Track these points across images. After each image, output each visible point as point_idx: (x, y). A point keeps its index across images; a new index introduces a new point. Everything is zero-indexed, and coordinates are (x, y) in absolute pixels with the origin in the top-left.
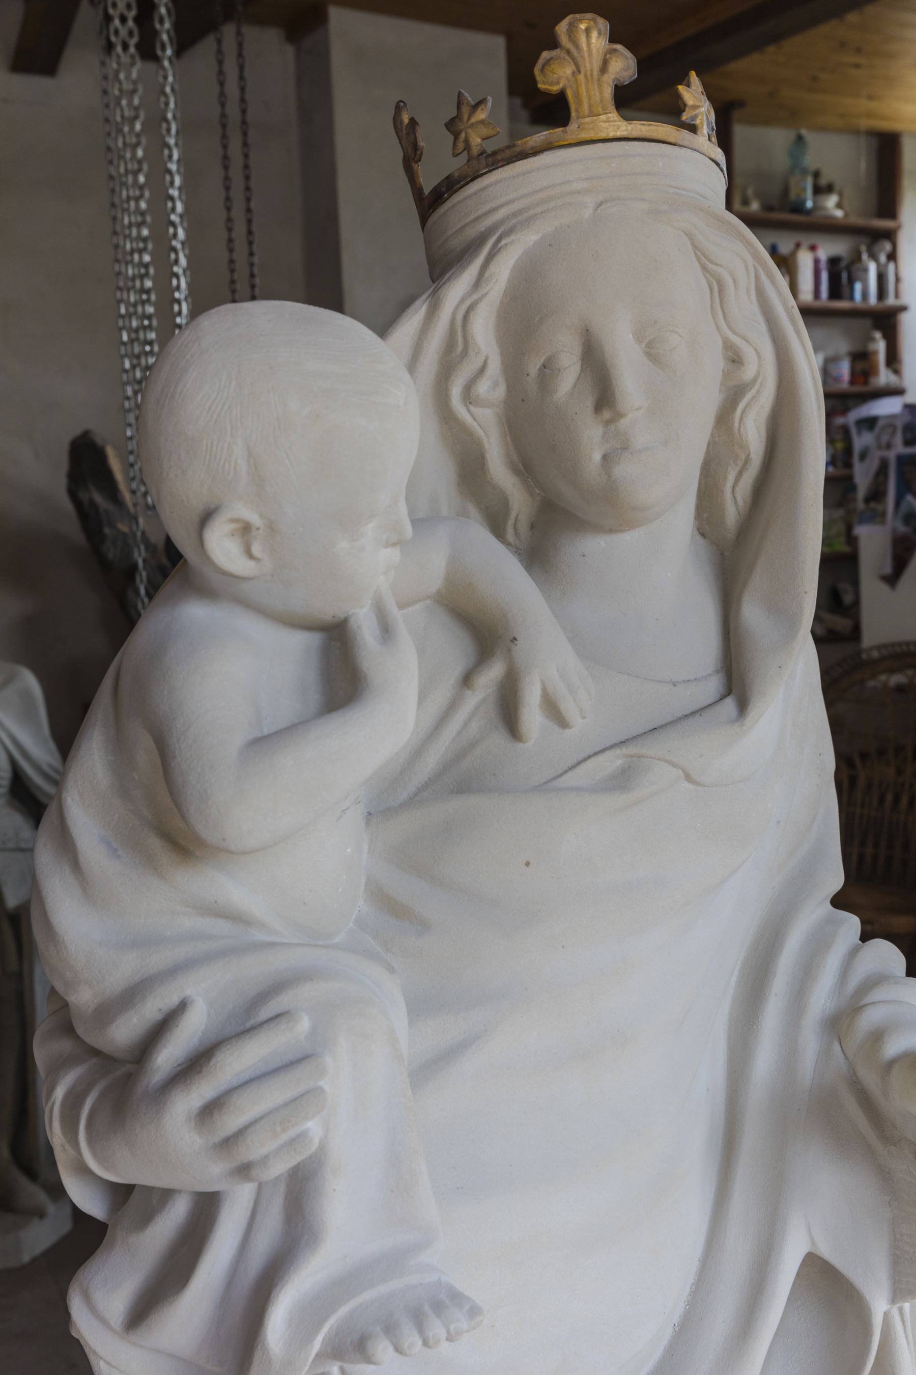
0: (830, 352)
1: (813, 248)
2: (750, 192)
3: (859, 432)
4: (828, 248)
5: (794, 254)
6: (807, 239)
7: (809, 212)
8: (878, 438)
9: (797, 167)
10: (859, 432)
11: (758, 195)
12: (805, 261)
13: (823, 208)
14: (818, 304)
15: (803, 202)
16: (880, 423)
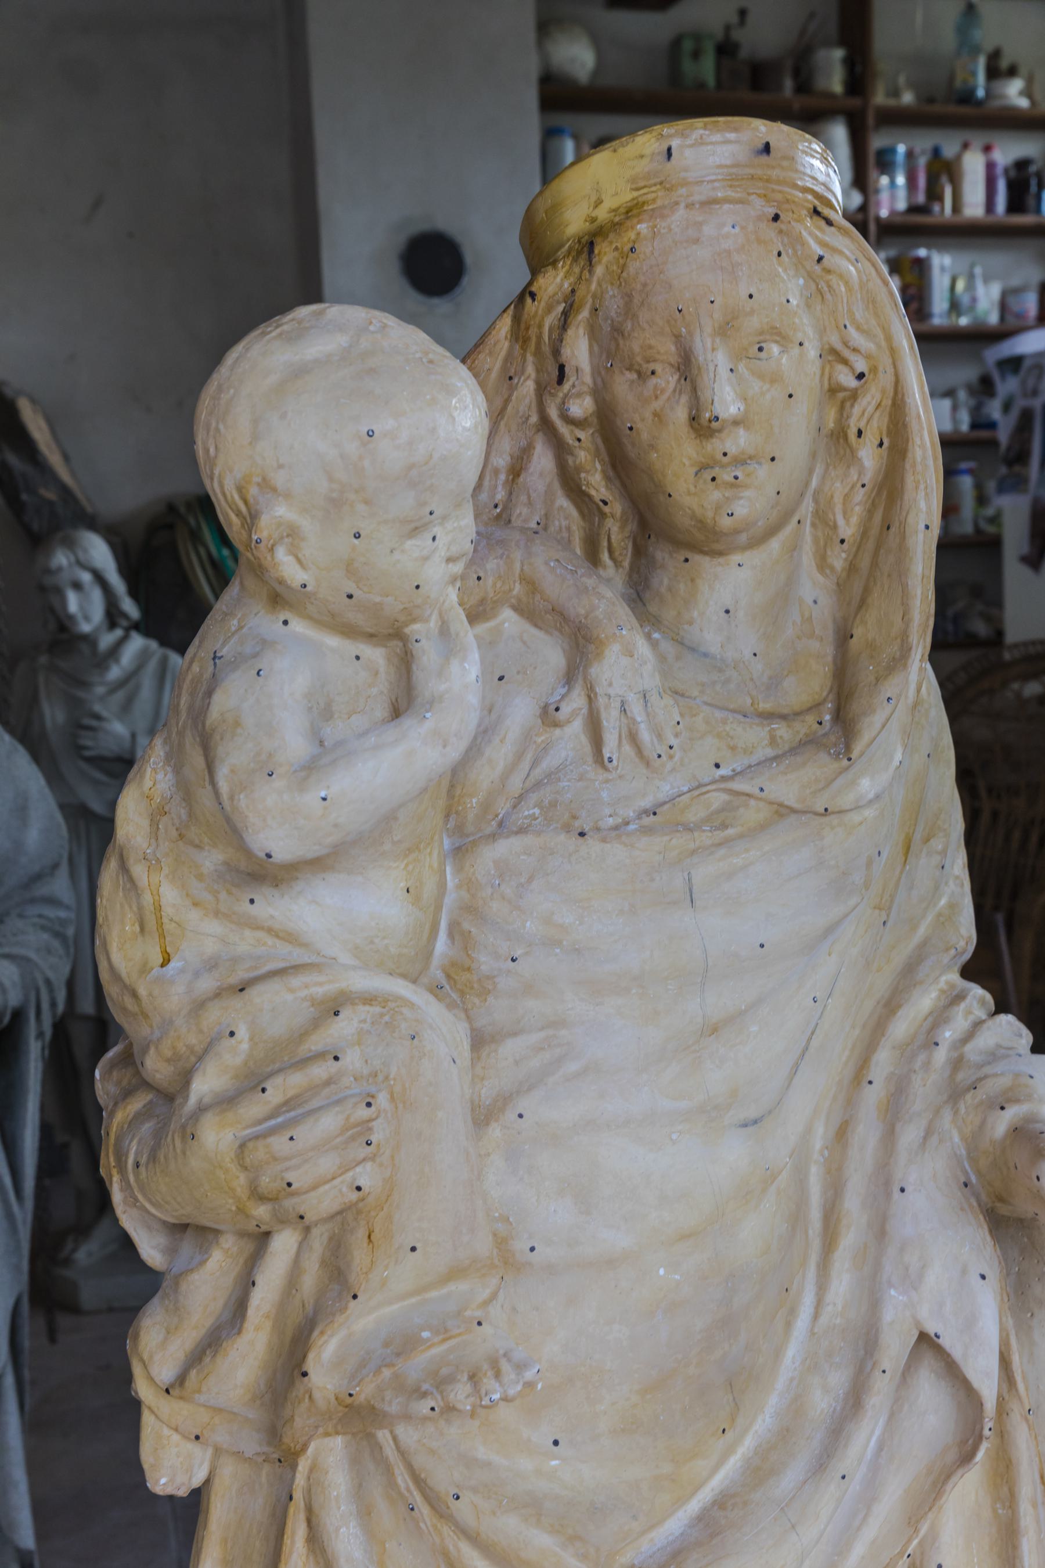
0: (1015, 282)
1: (987, 149)
2: (902, 80)
3: (1003, 377)
4: (1008, 151)
5: (959, 158)
6: (978, 139)
7: (979, 103)
8: (1023, 383)
9: (967, 46)
10: (1003, 377)
11: (912, 85)
12: (974, 165)
13: (1003, 96)
14: (991, 219)
15: (972, 91)
16: (1027, 364)
